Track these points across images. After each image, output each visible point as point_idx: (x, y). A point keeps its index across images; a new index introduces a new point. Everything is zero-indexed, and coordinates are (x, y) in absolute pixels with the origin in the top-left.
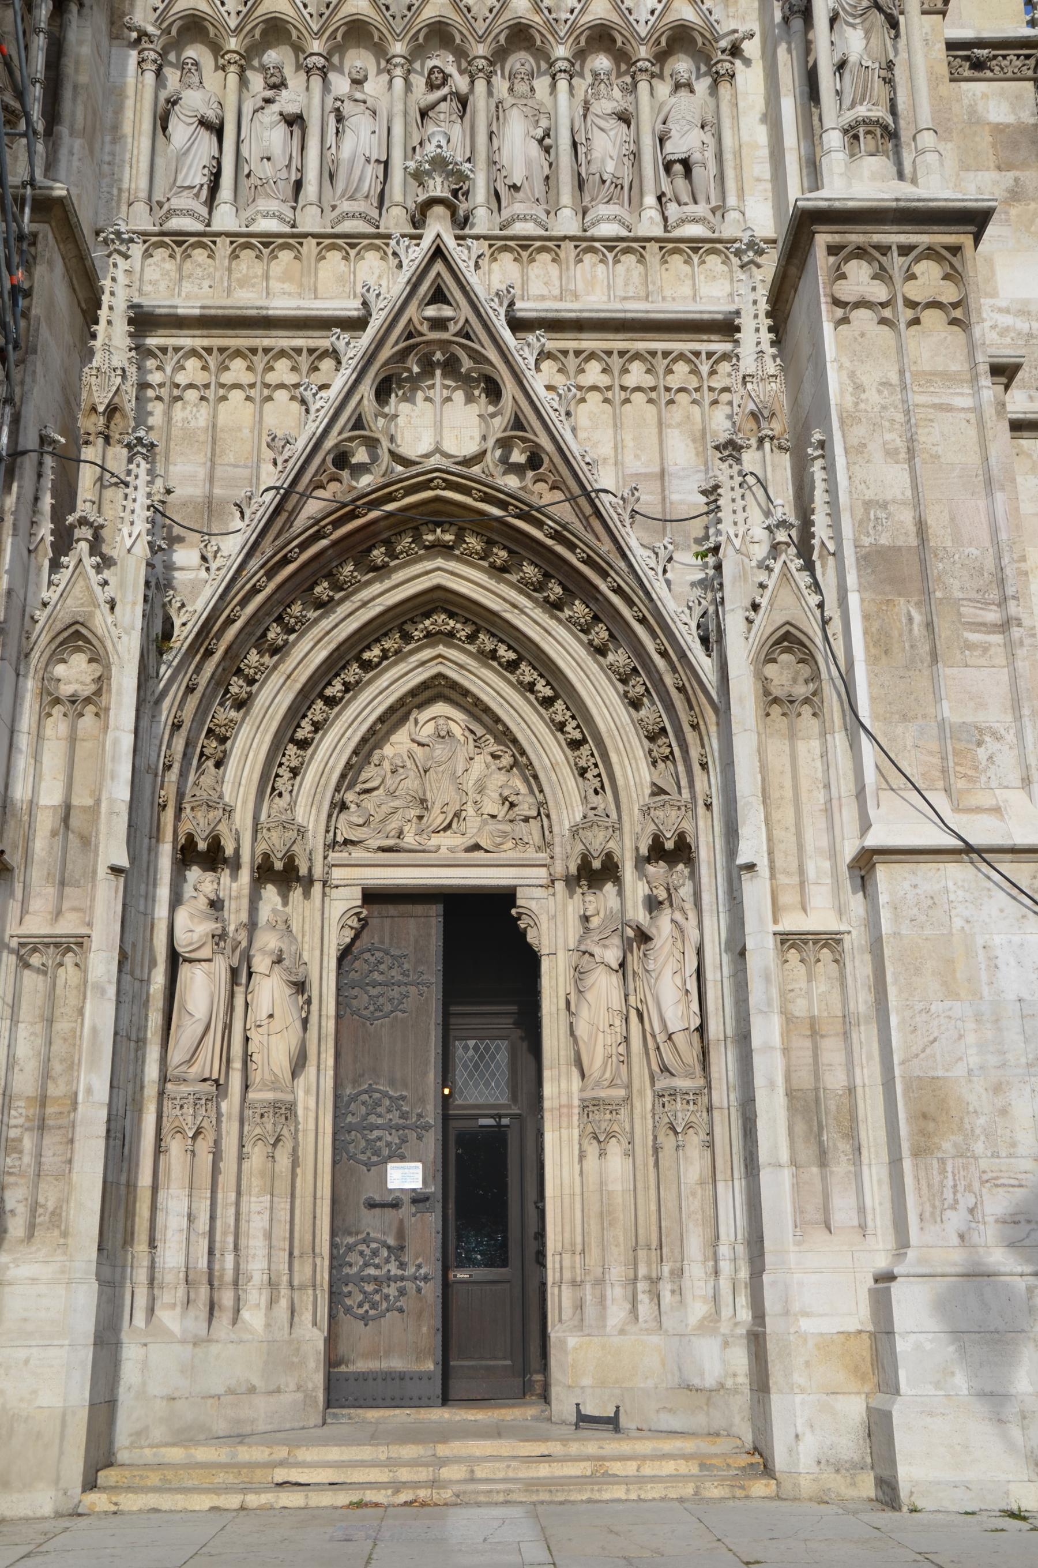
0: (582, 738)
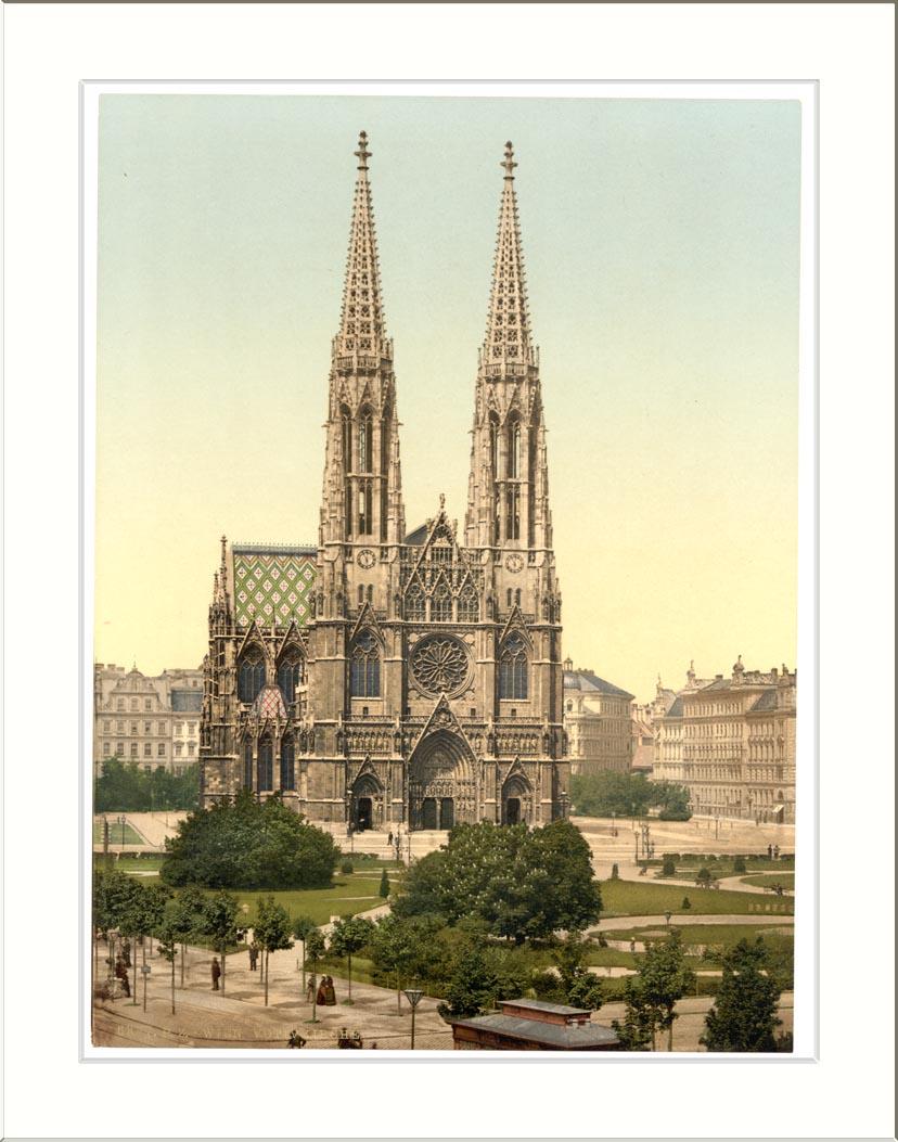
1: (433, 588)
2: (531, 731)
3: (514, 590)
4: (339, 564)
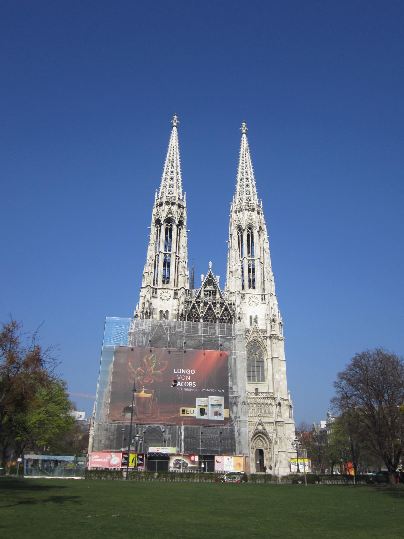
0: (266, 442)
1: (205, 313)
2: (269, 401)
3: (254, 317)
4: (148, 297)
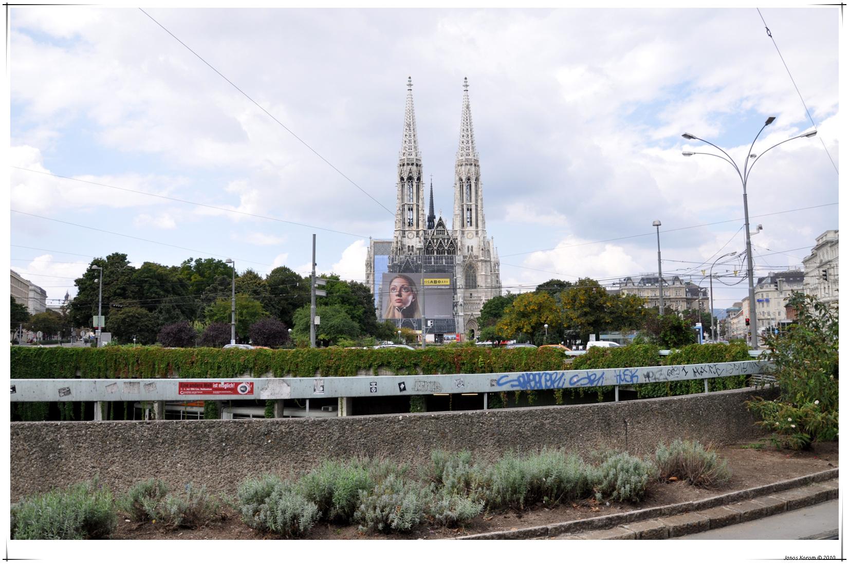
4: (399, 238)
